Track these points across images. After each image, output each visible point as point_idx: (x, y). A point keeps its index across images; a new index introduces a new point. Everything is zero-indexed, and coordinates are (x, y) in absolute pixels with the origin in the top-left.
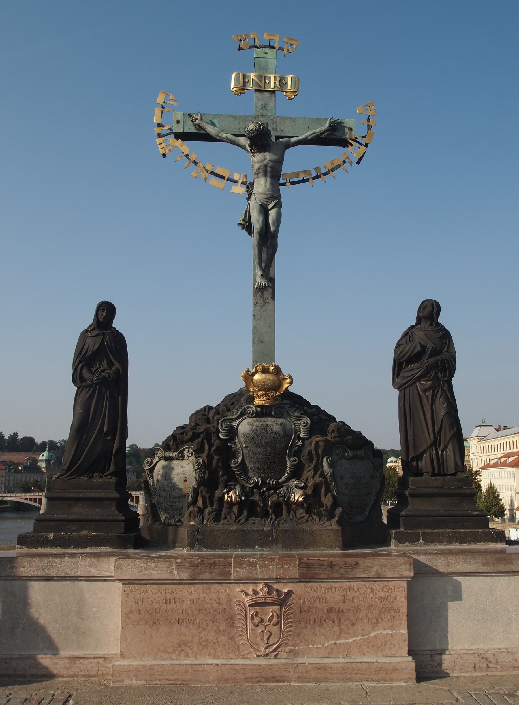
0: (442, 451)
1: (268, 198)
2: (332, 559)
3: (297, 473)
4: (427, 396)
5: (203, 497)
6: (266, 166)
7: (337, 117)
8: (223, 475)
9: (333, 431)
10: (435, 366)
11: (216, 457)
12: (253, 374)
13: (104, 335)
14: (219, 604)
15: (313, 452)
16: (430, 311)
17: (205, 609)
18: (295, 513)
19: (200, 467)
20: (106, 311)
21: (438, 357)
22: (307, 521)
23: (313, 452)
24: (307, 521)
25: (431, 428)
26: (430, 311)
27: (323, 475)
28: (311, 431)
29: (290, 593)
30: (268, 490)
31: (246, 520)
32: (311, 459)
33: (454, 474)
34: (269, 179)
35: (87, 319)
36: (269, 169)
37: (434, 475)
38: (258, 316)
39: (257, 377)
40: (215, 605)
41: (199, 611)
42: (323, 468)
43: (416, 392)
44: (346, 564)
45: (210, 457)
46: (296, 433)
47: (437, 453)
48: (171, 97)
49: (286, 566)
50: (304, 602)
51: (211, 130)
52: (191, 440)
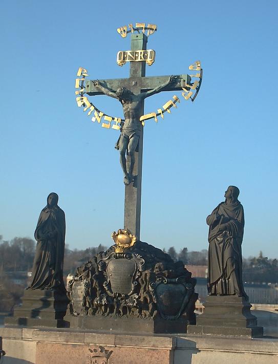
0: (228, 279)
1: (129, 132)
2: (131, 336)
3: (137, 291)
4: (220, 247)
5: (89, 302)
6: (129, 112)
7: (175, 73)
8: (99, 290)
9: (157, 268)
10: (226, 229)
11: (95, 281)
12: (117, 235)
13: (51, 212)
14: (79, 356)
15: (144, 280)
16: (233, 193)
17: (73, 358)
18: (133, 312)
19: (87, 285)
20: (53, 199)
21: (227, 224)
22: (138, 317)
23: (144, 280)
24: (138, 317)
25: (221, 267)
26: (233, 193)
27: (148, 292)
28: (145, 267)
29: (112, 352)
30: (122, 299)
31: (108, 315)
32: (143, 283)
33: (234, 294)
34: (131, 120)
35: (44, 204)
36: (131, 114)
37: (223, 295)
38: (127, 200)
39: (120, 237)
40: (78, 356)
41: (71, 359)
42: (149, 288)
43: (214, 245)
44: (138, 339)
45: (92, 281)
46: (137, 268)
47: (225, 280)
48: (85, 71)
49: (110, 338)
50: (119, 358)
51: (103, 89)
52: (84, 271)
